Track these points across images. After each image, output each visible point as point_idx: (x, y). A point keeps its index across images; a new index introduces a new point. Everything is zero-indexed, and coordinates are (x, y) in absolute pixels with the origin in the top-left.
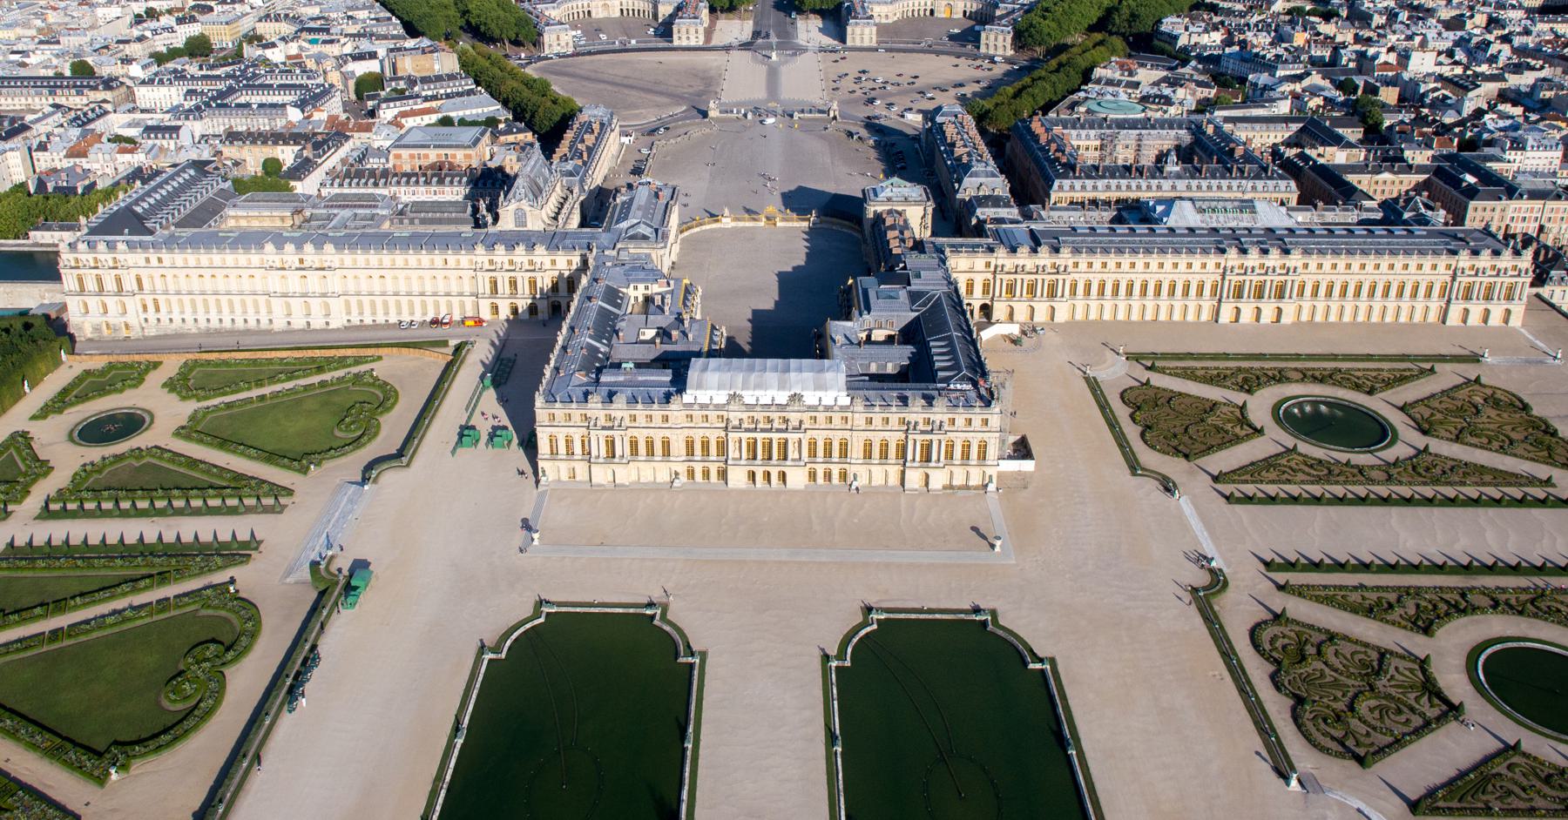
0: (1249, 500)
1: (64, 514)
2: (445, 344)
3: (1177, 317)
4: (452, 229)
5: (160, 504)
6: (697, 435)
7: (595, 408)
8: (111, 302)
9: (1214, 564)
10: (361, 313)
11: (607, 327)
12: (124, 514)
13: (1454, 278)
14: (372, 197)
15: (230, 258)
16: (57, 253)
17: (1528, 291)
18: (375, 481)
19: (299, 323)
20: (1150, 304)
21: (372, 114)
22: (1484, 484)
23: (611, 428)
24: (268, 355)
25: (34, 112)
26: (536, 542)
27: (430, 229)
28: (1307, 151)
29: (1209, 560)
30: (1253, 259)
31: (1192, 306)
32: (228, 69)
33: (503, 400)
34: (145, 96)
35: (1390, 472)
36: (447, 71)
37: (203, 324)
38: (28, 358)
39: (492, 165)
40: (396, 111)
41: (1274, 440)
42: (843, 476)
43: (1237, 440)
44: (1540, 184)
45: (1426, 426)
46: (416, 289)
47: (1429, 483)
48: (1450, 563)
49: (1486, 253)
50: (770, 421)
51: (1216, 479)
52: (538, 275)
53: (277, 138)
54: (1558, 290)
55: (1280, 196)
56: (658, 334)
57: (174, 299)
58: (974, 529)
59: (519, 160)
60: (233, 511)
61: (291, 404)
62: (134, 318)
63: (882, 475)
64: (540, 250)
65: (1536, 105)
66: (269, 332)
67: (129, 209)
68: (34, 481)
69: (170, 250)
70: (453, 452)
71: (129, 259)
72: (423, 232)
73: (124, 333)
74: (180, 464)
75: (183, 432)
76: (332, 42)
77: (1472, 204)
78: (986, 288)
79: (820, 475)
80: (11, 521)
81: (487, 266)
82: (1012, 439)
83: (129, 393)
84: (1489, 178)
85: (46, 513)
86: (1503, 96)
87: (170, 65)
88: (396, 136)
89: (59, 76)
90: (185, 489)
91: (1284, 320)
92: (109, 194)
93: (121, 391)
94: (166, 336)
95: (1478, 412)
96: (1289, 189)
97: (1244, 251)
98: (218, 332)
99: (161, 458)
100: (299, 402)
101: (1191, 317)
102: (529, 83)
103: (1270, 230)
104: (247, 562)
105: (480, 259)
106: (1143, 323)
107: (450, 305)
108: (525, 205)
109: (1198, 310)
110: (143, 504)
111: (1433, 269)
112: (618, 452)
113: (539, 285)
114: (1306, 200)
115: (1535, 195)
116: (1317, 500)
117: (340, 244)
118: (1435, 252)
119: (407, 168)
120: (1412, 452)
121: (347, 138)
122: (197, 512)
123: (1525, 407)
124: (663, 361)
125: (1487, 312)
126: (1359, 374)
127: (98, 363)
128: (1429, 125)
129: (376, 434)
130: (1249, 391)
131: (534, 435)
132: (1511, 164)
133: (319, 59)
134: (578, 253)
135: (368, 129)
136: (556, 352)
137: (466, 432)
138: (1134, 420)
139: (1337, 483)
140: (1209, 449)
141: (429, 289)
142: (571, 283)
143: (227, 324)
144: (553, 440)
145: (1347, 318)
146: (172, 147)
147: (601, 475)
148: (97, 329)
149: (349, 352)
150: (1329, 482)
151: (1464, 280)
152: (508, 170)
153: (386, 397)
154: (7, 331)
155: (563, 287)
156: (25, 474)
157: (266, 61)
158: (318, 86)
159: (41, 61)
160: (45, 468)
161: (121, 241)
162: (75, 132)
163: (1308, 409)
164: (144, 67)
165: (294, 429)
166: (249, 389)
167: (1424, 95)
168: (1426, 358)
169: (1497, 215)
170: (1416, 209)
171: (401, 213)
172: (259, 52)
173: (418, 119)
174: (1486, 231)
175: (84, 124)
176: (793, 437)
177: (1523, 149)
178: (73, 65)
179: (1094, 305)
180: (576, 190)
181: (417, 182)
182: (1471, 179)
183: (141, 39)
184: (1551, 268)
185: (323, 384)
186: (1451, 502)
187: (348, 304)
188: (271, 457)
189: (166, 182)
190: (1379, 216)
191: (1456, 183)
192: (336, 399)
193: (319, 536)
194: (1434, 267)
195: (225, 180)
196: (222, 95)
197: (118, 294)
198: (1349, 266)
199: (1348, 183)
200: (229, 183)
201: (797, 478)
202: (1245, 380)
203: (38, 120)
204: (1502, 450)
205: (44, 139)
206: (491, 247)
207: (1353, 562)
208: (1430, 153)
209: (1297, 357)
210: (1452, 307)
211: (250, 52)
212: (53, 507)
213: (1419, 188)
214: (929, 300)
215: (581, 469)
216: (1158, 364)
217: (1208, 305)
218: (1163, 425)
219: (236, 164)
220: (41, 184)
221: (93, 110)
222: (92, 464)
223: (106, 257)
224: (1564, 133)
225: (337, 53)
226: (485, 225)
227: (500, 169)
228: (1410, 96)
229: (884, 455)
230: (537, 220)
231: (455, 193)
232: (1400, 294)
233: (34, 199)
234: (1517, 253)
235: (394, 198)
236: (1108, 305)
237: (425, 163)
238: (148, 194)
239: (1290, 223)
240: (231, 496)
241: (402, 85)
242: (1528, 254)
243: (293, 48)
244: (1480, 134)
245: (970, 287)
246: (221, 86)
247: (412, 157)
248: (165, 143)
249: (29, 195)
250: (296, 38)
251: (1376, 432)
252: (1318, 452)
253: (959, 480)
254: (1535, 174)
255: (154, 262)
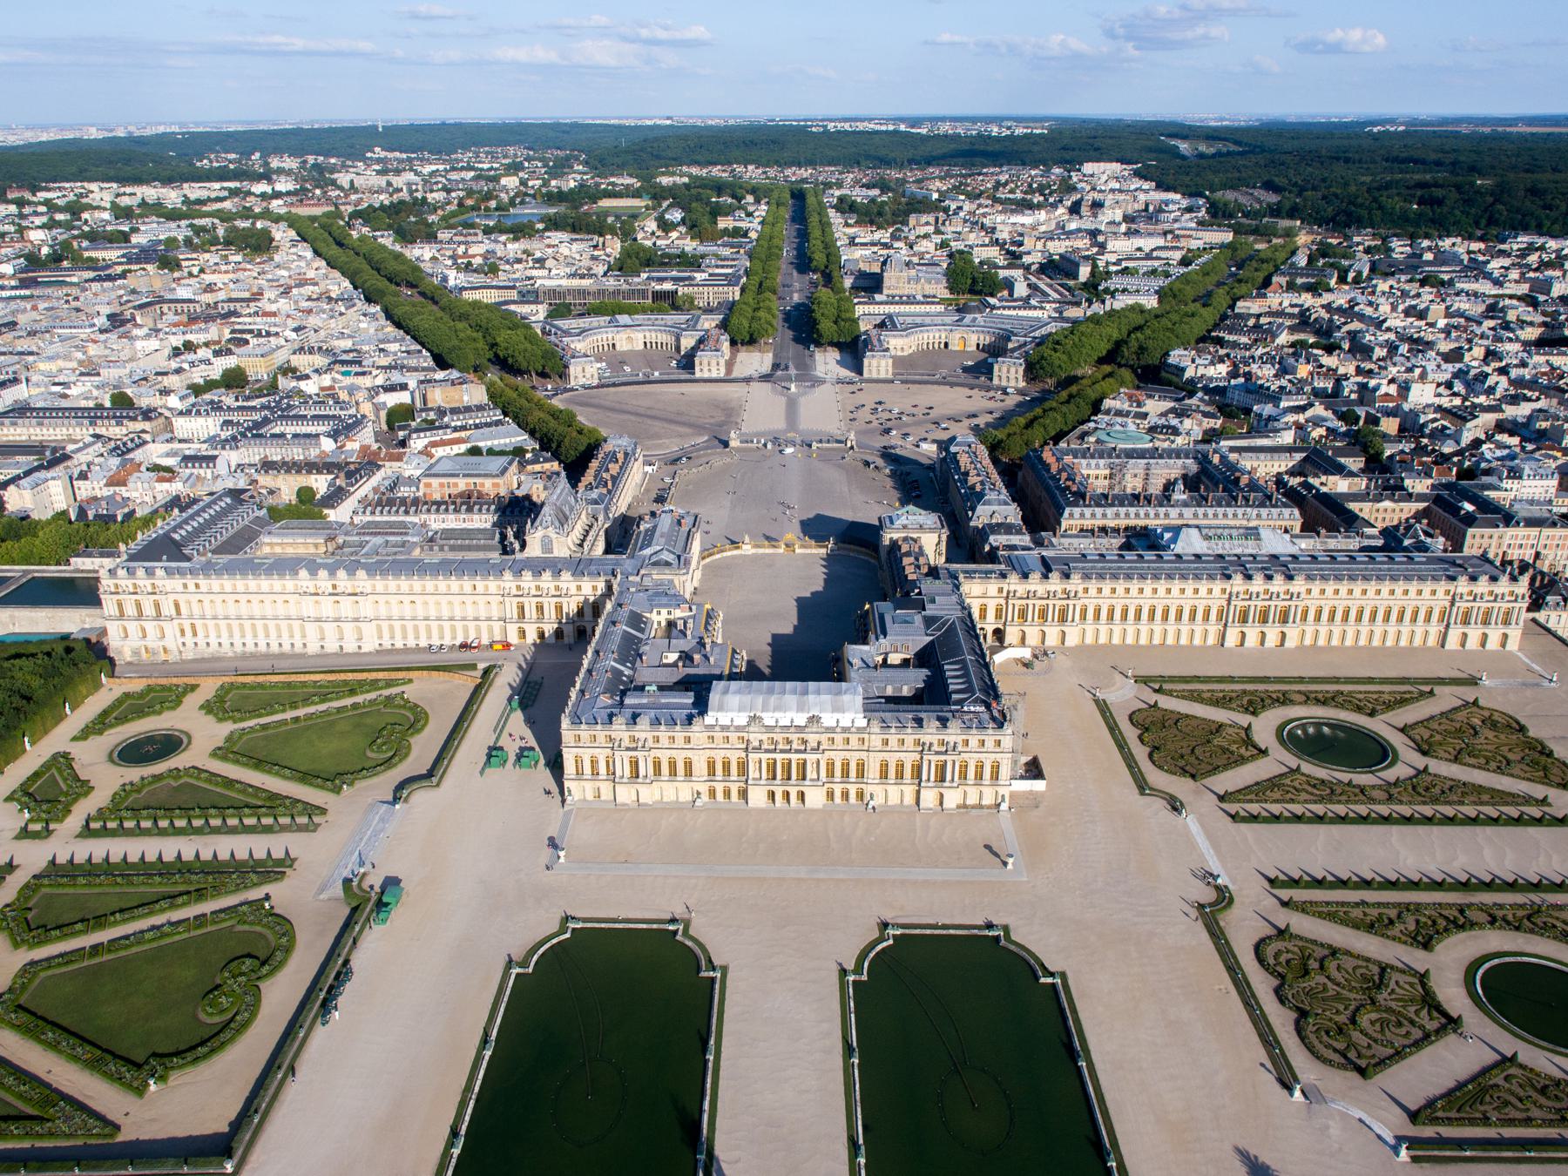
0: (1254, 818)
1: (104, 832)
2: (473, 667)
3: (1184, 641)
4: (481, 555)
5: (197, 823)
6: (719, 756)
7: (619, 730)
8: (150, 626)
9: (1219, 881)
10: (392, 638)
11: (631, 650)
12: (162, 833)
13: (1452, 603)
14: (403, 525)
15: (265, 584)
16: (97, 579)
17: (1525, 616)
18: (406, 800)
19: (332, 647)
20: (1158, 628)
21: (403, 444)
22: (1482, 803)
23: (635, 749)
24: (303, 678)
25: (76, 442)
26: (562, 860)
27: (459, 556)
28: (1311, 480)
29: (1215, 877)
30: (1258, 584)
31: (1199, 630)
32: (263, 400)
33: (530, 722)
34: (183, 426)
35: (1391, 791)
36: (476, 402)
37: (239, 648)
38: (69, 681)
39: (519, 493)
40: (426, 441)
41: (1278, 760)
42: (860, 795)
43: (1242, 760)
44: (1536, 512)
45: (1425, 747)
46: (446, 614)
47: (1428, 802)
48: (1449, 880)
49: (1484, 579)
50: (789, 742)
51: (1222, 798)
52: (564, 600)
53: (311, 467)
54: (1554, 615)
55: (1284, 523)
56: (680, 658)
57: (211, 623)
58: (987, 847)
59: (545, 488)
60: (268, 830)
61: (324, 725)
62: (172, 641)
63: (897, 794)
64: (566, 576)
65: (1535, 436)
66: (302, 656)
67: (167, 536)
68: (75, 800)
69: (207, 576)
70: (482, 772)
71: (167, 585)
72: (452, 559)
73: (163, 657)
74: (217, 784)
75: (220, 753)
76: (364, 374)
77: (1470, 531)
78: (998, 615)
79: (838, 794)
80: (52, 839)
81: (514, 592)
82: (1024, 759)
83: (167, 715)
84: (1486, 506)
85: (87, 832)
86: (1501, 427)
87: (207, 397)
88: (426, 466)
89: (100, 407)
90: (222, 808)
91: (1287, 644)
92: (148, 521)
93: (160, 713)
94: (203, 660)
95: (1476, 733)
96: (1292, 517)
97: (1249, 577)
98: (253, 656)
99: (198, 778)
100: (332, 724)
101: (1197, 641)
102: (555, 414)
103: (1275, 557)
104: (282, 879)
105: (507, 585)
106: (1151, 647)
107: (478, 629)
108: (551, 532)
109: (1204, 634)
110: (181, 823)
111: (1432, 594)
112: (642, 772)
113: (565, 610)
114: (1309, 528)
115: (1532, 522)
116: (1320, 819)
117: (372, 570)
118: (1434, 578)
119: (437, 497)
120: (1412, 772)
121: (379, 467)
122: (233, 831)
123: (1522, 729)
124: (685, 684)
125: (1485, 636)
126: (1361, 696)
127: (137, 686)
128: (1428, 455)
129: (407, 755)
130: (1254, 714)
131: (560, 755)
132: (1509, 492)
133: (351, 390)
134: (602, 579)
135: (399, 458)
136: (582, 674)
137: (494, 753)
138: (1142, 741)
139: (1339, 802)
140: (1215, 770)
141: (458, 614)
142: (596, 608)
143: (262, 648)
144: (578, 761)
145: (1349, 642)
146: (209, 476)
147: (625, 794)
148: (136, 653)
149: (380, 675)
150: (1331, 802)
151: (1462, 605)
152: (535, 498)
153: (416, 719)
154: (49, 654)
155: (588, 612)
156: (67, 794)
157: (300, 393)
158: (351, 416)
159: (82, 392)
160: (85, 788)
161: (159, 567)
162: (114, 462)
163: (1311, 730)
164: (182, 398)
165: (327, 750)
166: (284, 711)
167: (1424, 425)
168: (1426, 681)
169: (1494, 542)
170: (1415, 536)
171: (431, 540)
172: (294, 384)
173: (448, 448)
174: (1484, 558)
175: (124, 453)
176: (811, 758)
177: (1520, 477)
178: (113, 396)
179: (1104, 629)
180: (601, 518)
181: (447, 510)
182: (1468, 507)
183: (179, 371)
184: (1547, 593)
185: (355, 706)
186: (1451, 821)
187: (379, 629)
188: (305, 777)
189: (203, 510)
190: (1380, 543)
191: (1455, 510)
192: (369, 721)
193: (352, 853)
194: (1434, 592)
195: (260, 507)
196: (257, 425)
197: (158, 619)
198: (1350, 592)
199: (1350, 511)
200: (264, 511)
201: (816, 797)
202: (1250, 702)
203: (79, 450)
204: (1499, 770)
205: (85, 468)
206: (518, 573)
207: (1355, 879)
208: (1429, 482)
209: (1301, 680)
210: (1451, 631)
211: (285, 383)
212: (93, 825)
213: (1418, 516)
214: (944, 624)
215: (606, 789)
216: (1165, 686)
217: (1214, 629)
218: (1170, 746)
219: (271, 492)
220: (82, 512)
221: (132, 440)
222: (132, 784)
223: (144, 583)
224: (1559, 462)
225: (369, 385)
226: (513, 552)
227: (528, 497)
228: (1410, 427)
229: (900, 775)
230: (563, 547)
231: (483, 520)
232: (1401, 619)
233: (75, 526)
234: (1514, 579)
235: (424, 525)
236: (1117, 630)
237: (454, 491)
238: (186, 522)
239: (1294, 550)
240: (266, 815)
241: (432, 415)
242: (1525, 580)
243: (326, 380)
244: (1478, 463)
245: (983, 612)
246: (257, 417)
247: (442, 485)
248: (202, 472)
249: (70, 522)
250: (329, 369)
251: (1380, 753)
252: (1321, 772)
253: (972, 800)
254: (1531, 502)
255: (192, 587)
